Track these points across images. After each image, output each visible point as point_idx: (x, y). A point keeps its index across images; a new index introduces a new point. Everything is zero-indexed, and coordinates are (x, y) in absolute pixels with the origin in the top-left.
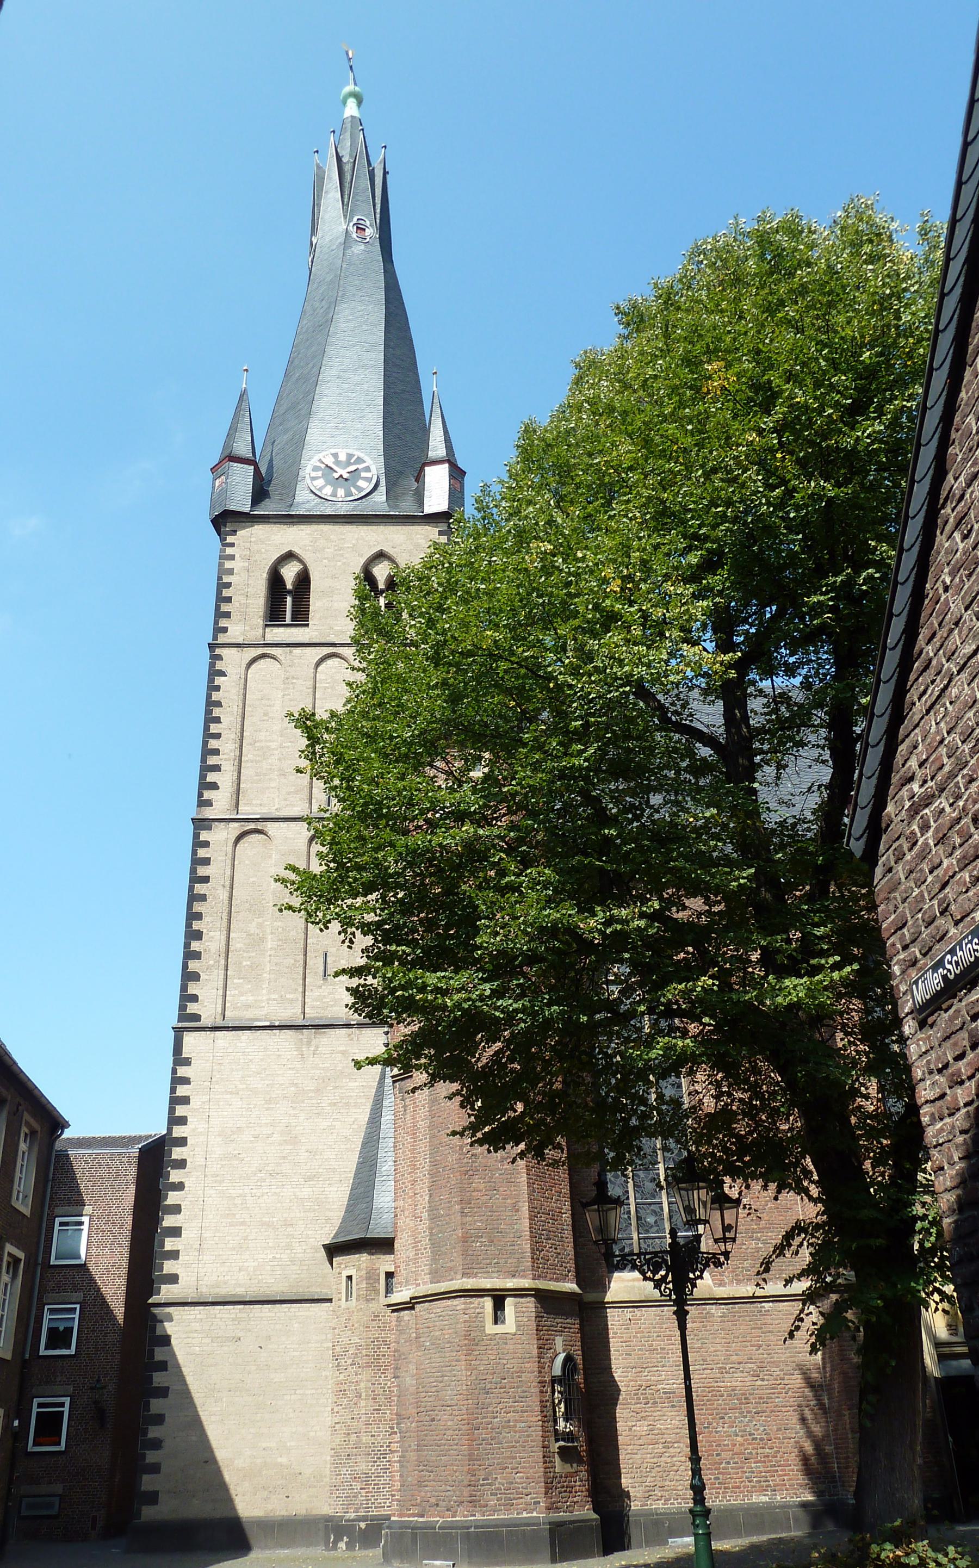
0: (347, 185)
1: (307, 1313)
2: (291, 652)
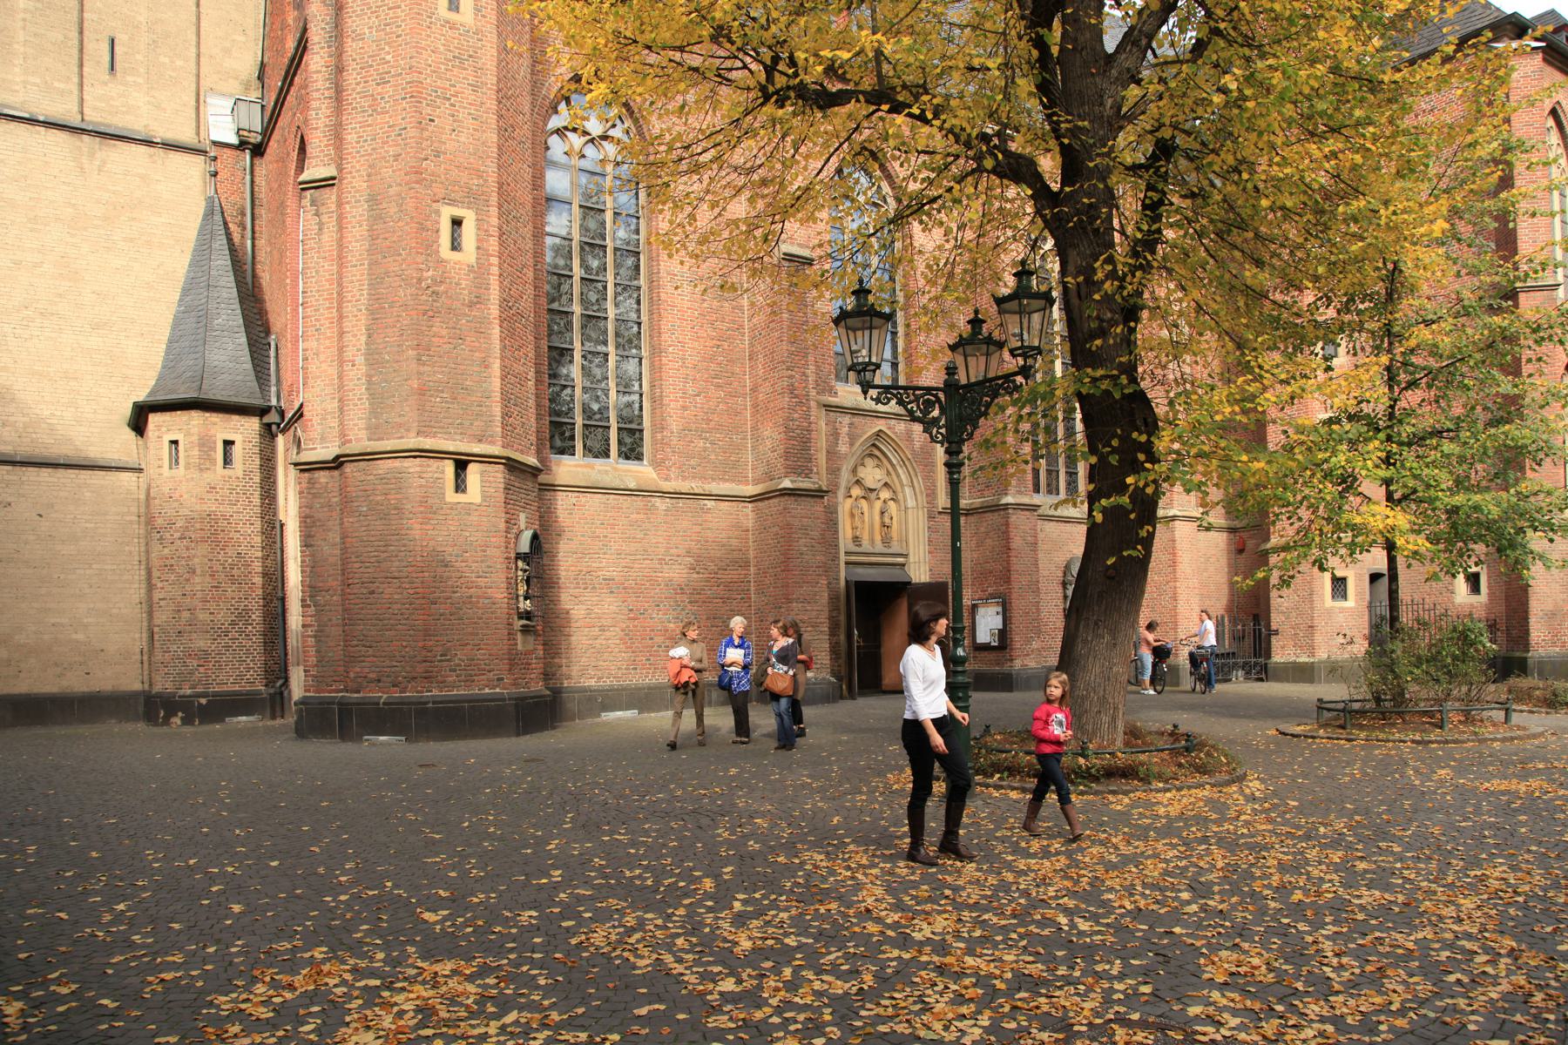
1: (102, 482)
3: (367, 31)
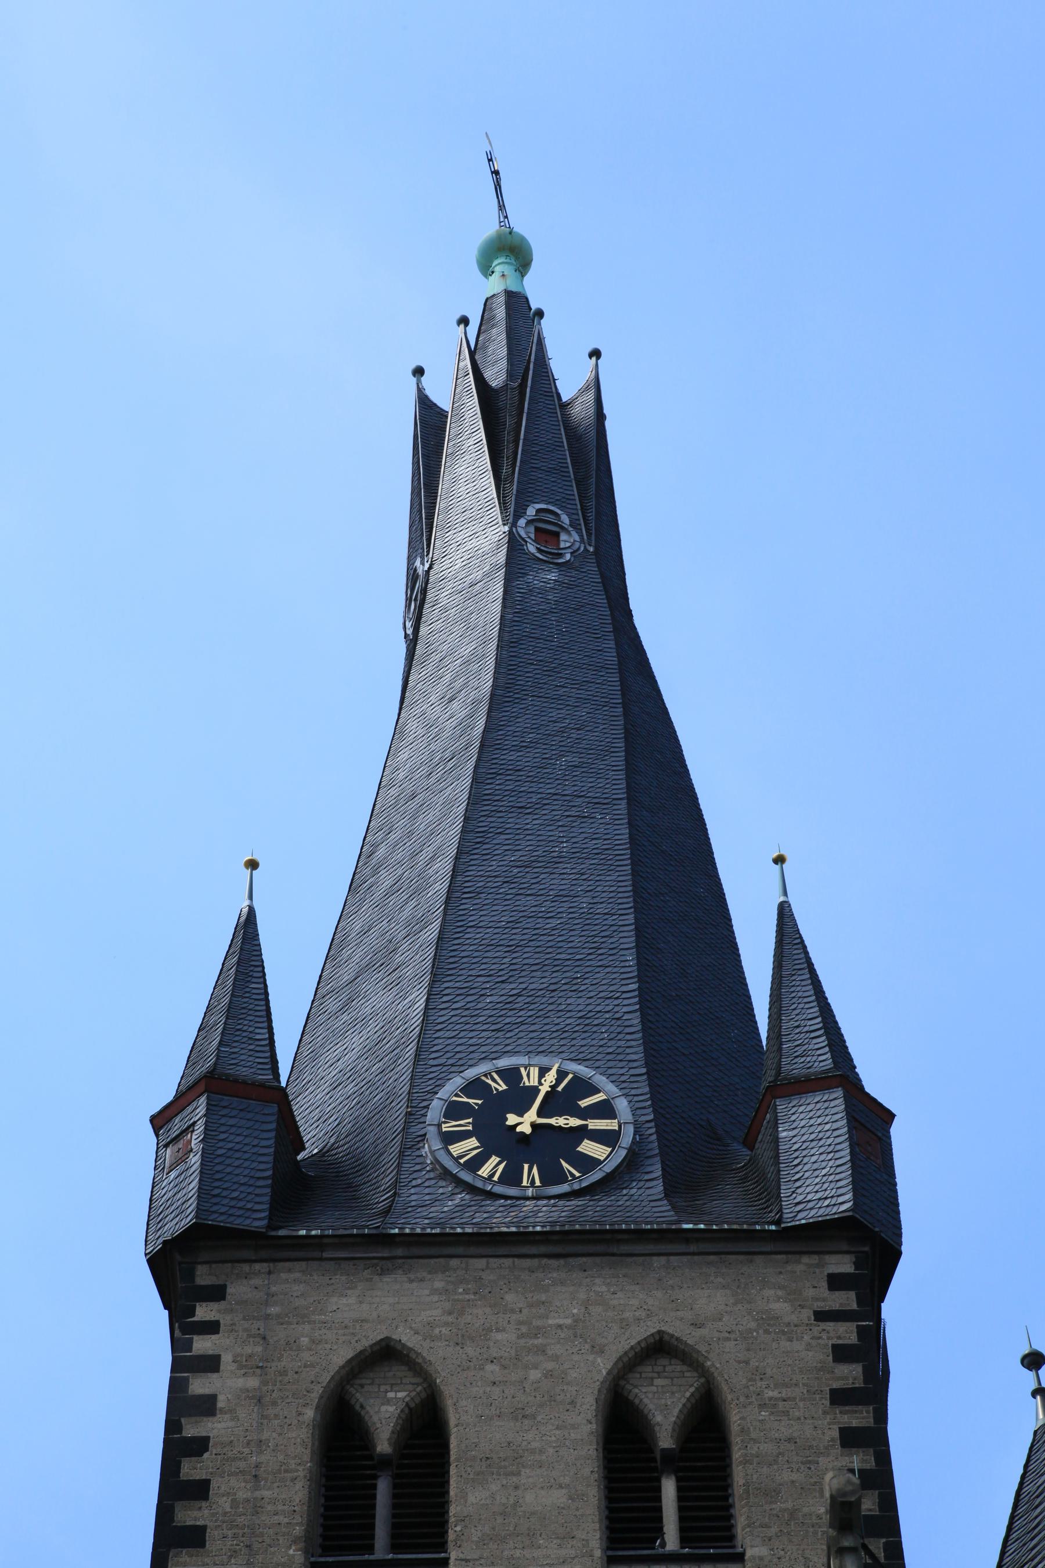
0: (507, 437)
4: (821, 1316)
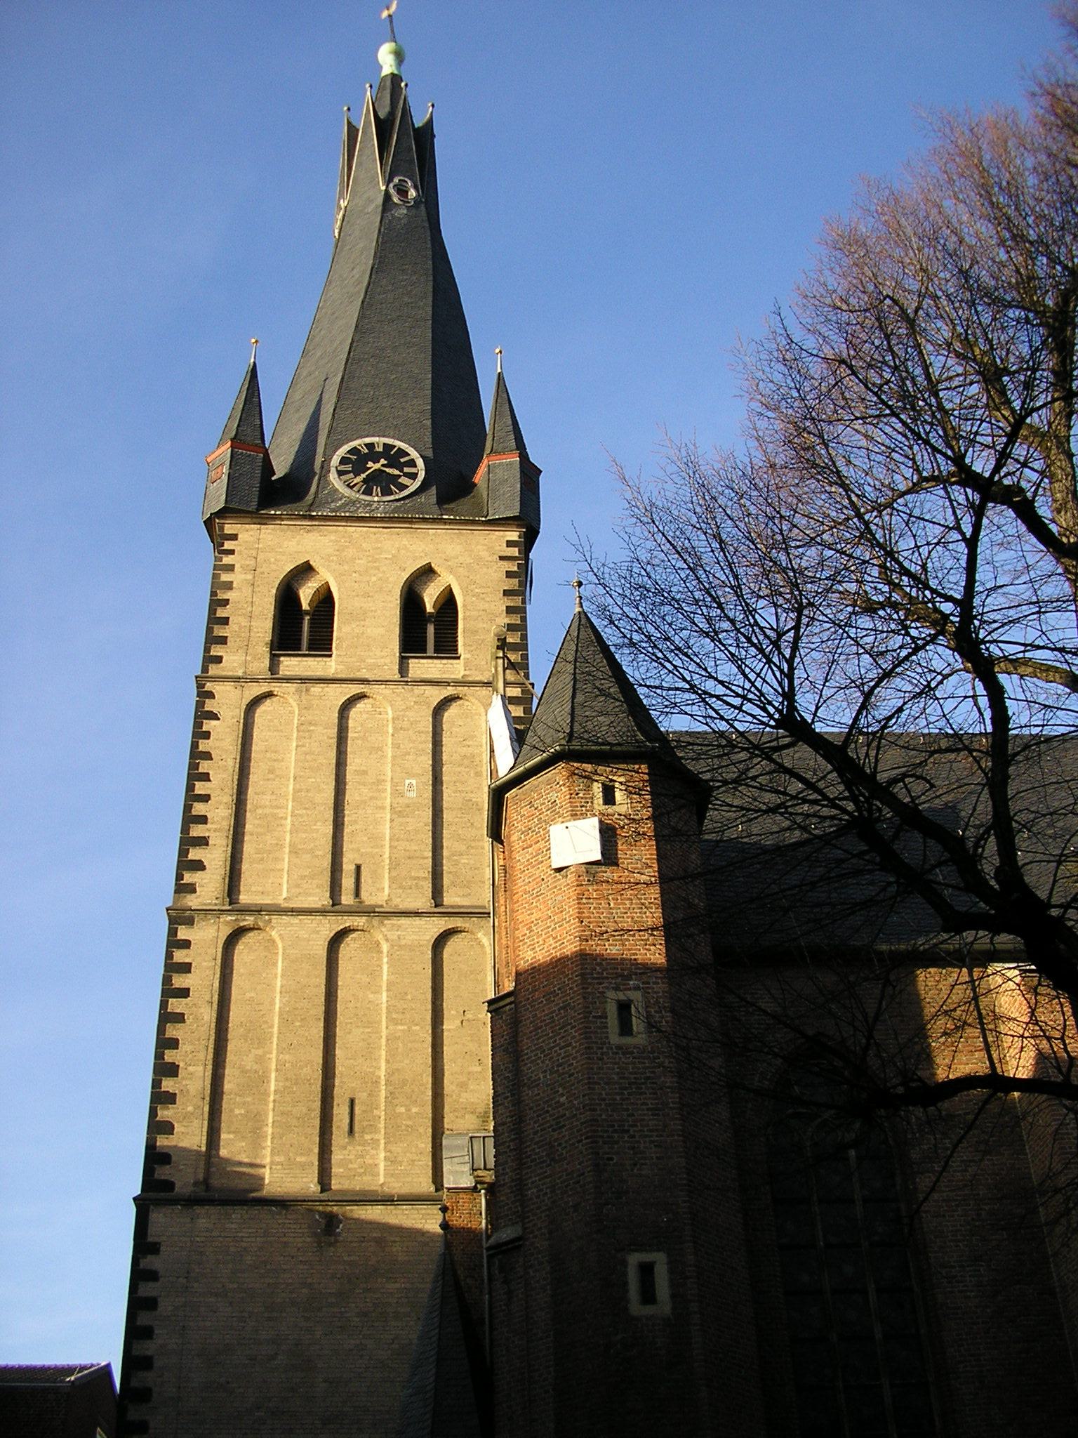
2: (307, 690)
3: (541, 1076)
4: (502, 558)
